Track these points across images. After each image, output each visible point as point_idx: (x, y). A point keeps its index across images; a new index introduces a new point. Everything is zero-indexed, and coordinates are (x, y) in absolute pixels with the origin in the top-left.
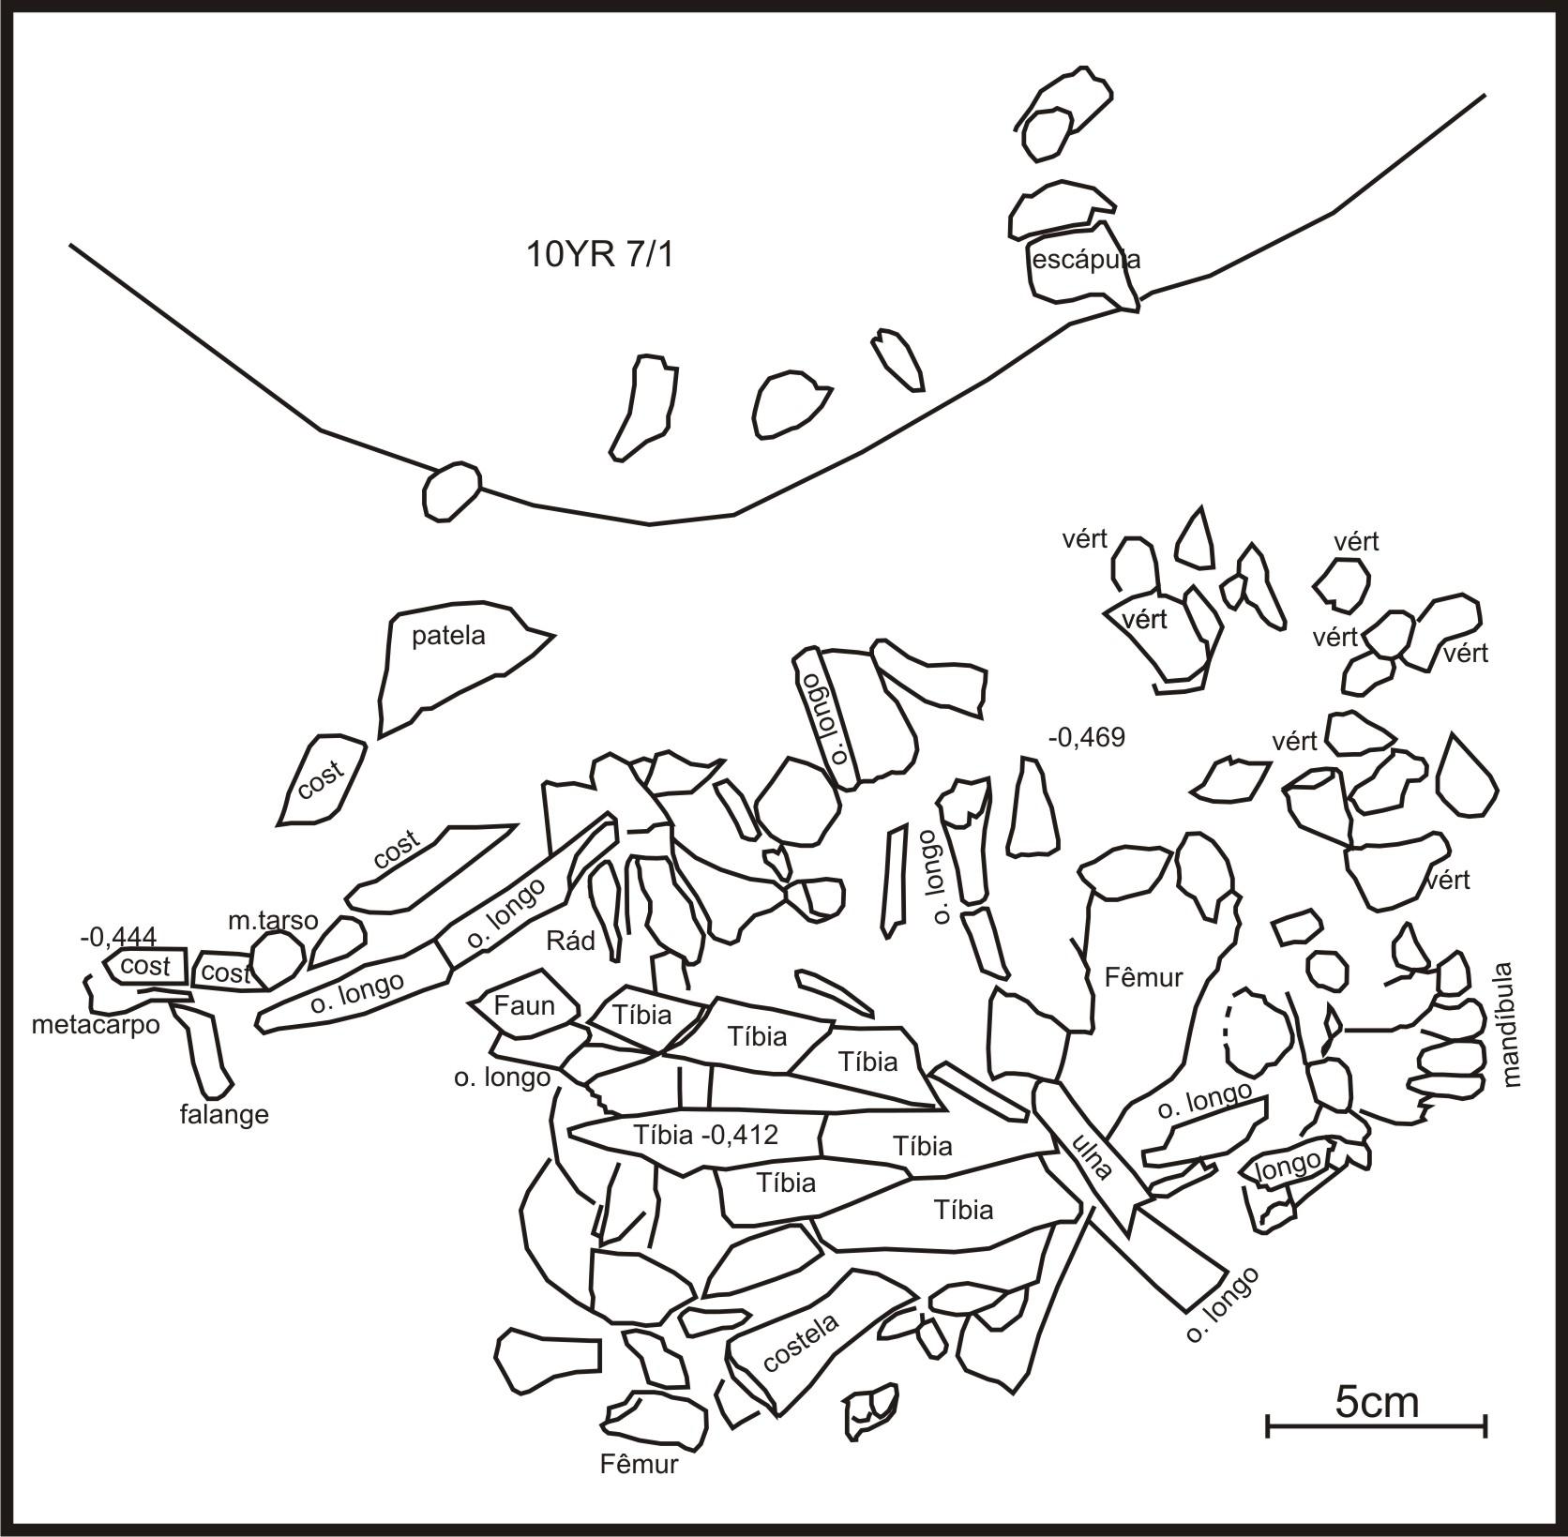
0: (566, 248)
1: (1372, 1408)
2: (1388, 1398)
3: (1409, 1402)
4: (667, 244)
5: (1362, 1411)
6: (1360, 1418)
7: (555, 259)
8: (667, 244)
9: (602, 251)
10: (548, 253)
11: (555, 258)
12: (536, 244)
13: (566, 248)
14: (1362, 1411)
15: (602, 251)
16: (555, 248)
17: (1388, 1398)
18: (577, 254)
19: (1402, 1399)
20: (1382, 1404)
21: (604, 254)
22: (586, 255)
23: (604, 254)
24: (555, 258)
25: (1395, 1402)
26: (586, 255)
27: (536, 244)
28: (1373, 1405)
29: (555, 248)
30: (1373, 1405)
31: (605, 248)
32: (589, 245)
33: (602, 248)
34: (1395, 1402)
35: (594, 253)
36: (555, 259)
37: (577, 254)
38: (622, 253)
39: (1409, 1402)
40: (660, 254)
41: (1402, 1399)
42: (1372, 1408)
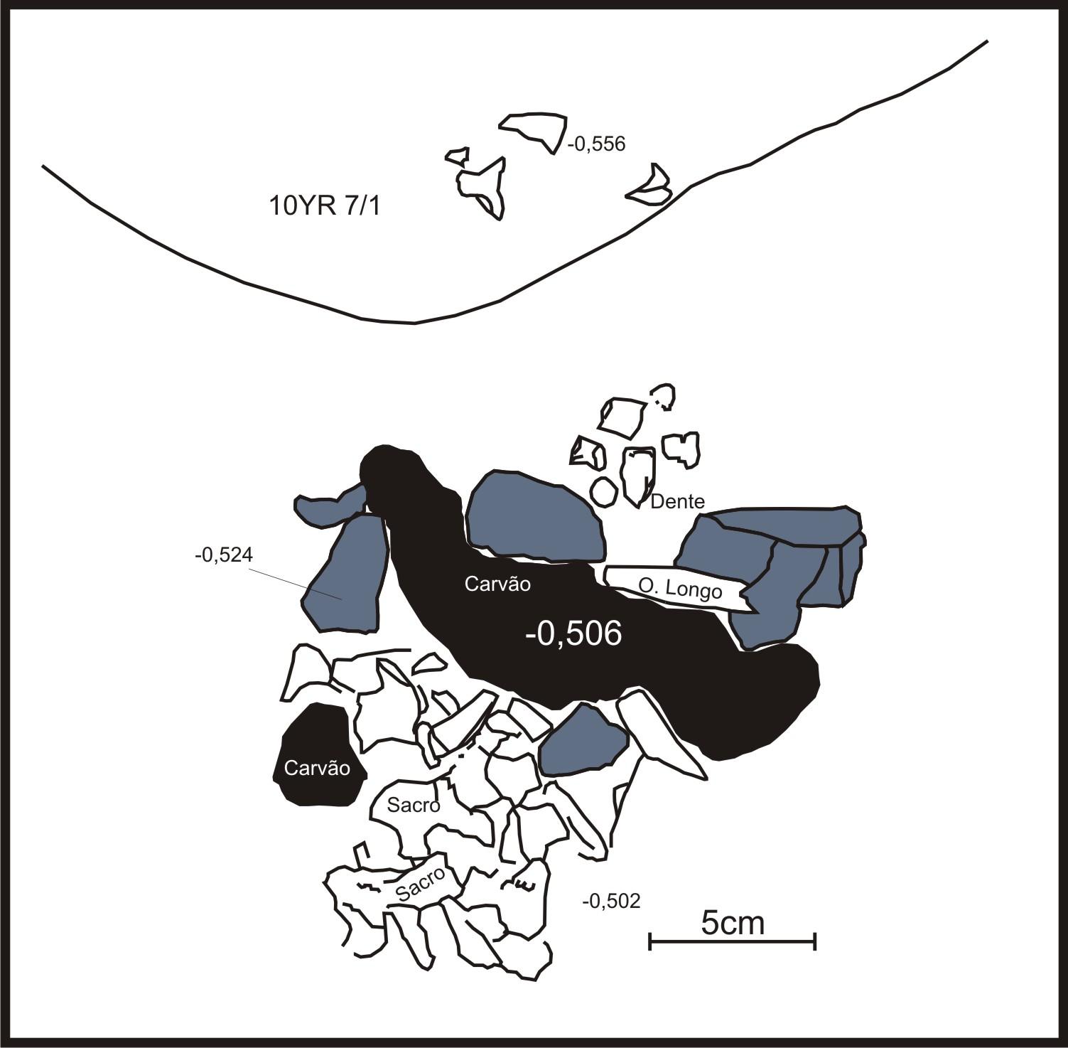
0: (299, 200)
4: (376, 198)
7: (290, 209)
8: (376, 198)
9: (326, 203)
10: (285, 204)
11: (290, 208)
12: (276, 198)
13: (299, 200)
15: (326, 203)
16: (290, 200)
18: (307, 205)
21: (328, 205)
22: (314, 206)
23: (328, 205)
24: (290, 208)
26: (314, 206)
27: (276, 198)
29: (290, 200)
31: (328, 200)
32: (317, 199)
33: (326, 200)
35: (321, 205)
36: (290, 209)
37: (307, 205)
38: (341, 205)
40: (370, 206)
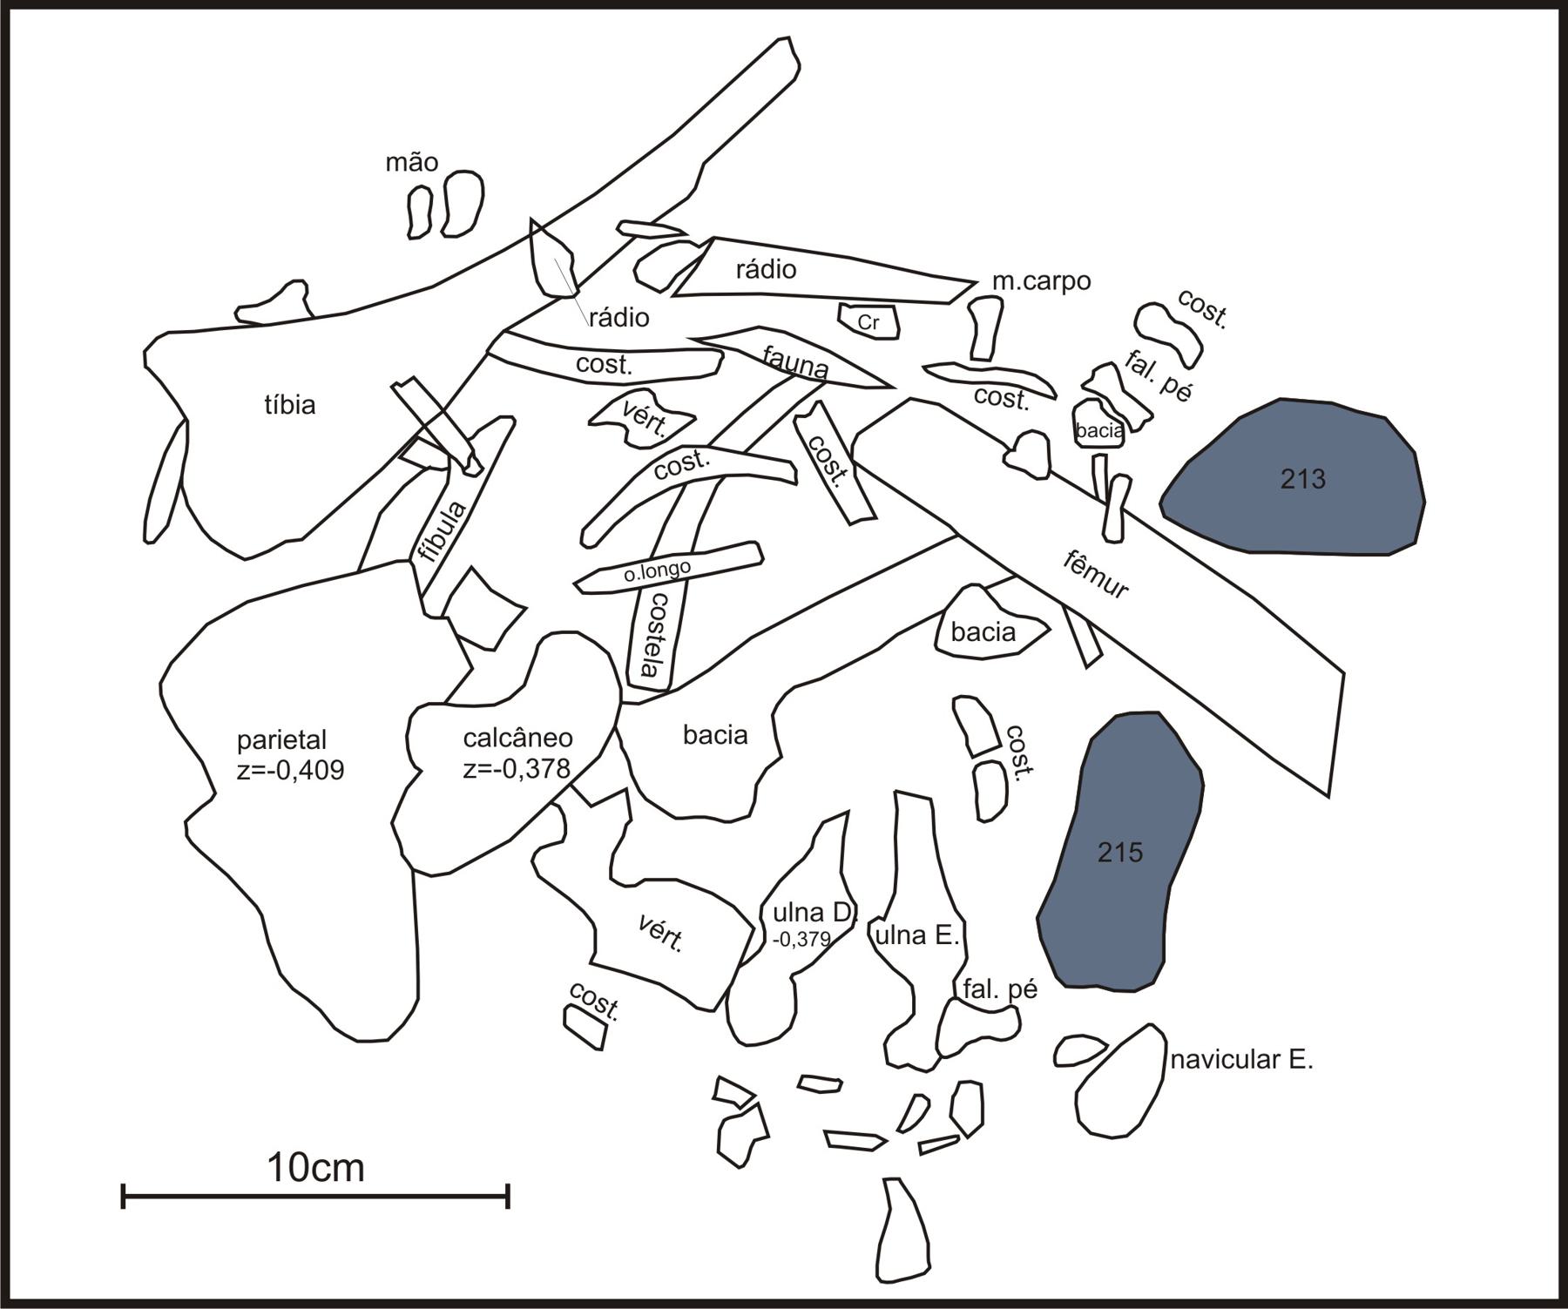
1: (321, 1175)
2: (336, 1164)
3: (355, 1167)
5: (314, 1177)
6: (310, 1186)
14: (314, 1177)
17: (336, 1164)
19: (349, 1165)
20: (331, 1170)
25: (342, 1168)
28: (322, 1170)
30: (322, 1170)
34: (342, 1168)
39: (355, 1167)
41: (349, 1165)
42: (321, 1175)
